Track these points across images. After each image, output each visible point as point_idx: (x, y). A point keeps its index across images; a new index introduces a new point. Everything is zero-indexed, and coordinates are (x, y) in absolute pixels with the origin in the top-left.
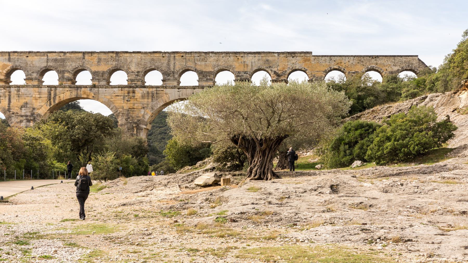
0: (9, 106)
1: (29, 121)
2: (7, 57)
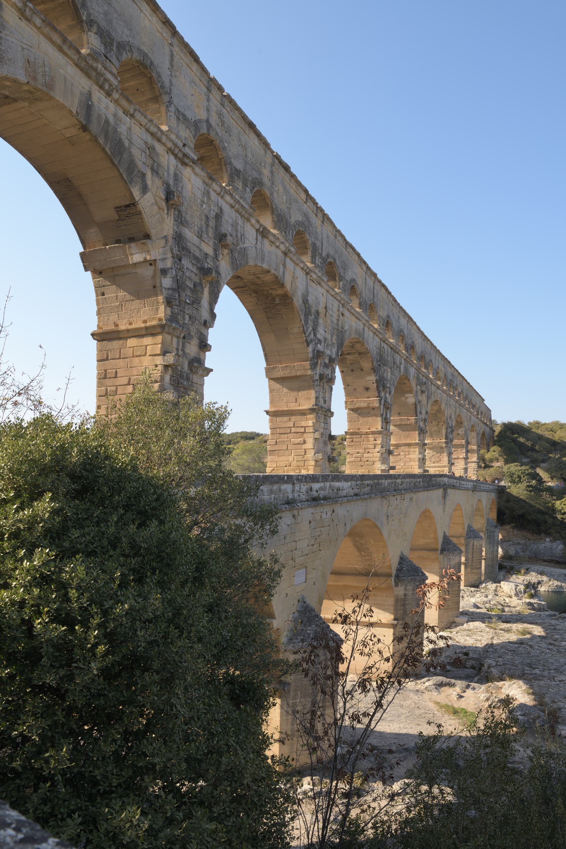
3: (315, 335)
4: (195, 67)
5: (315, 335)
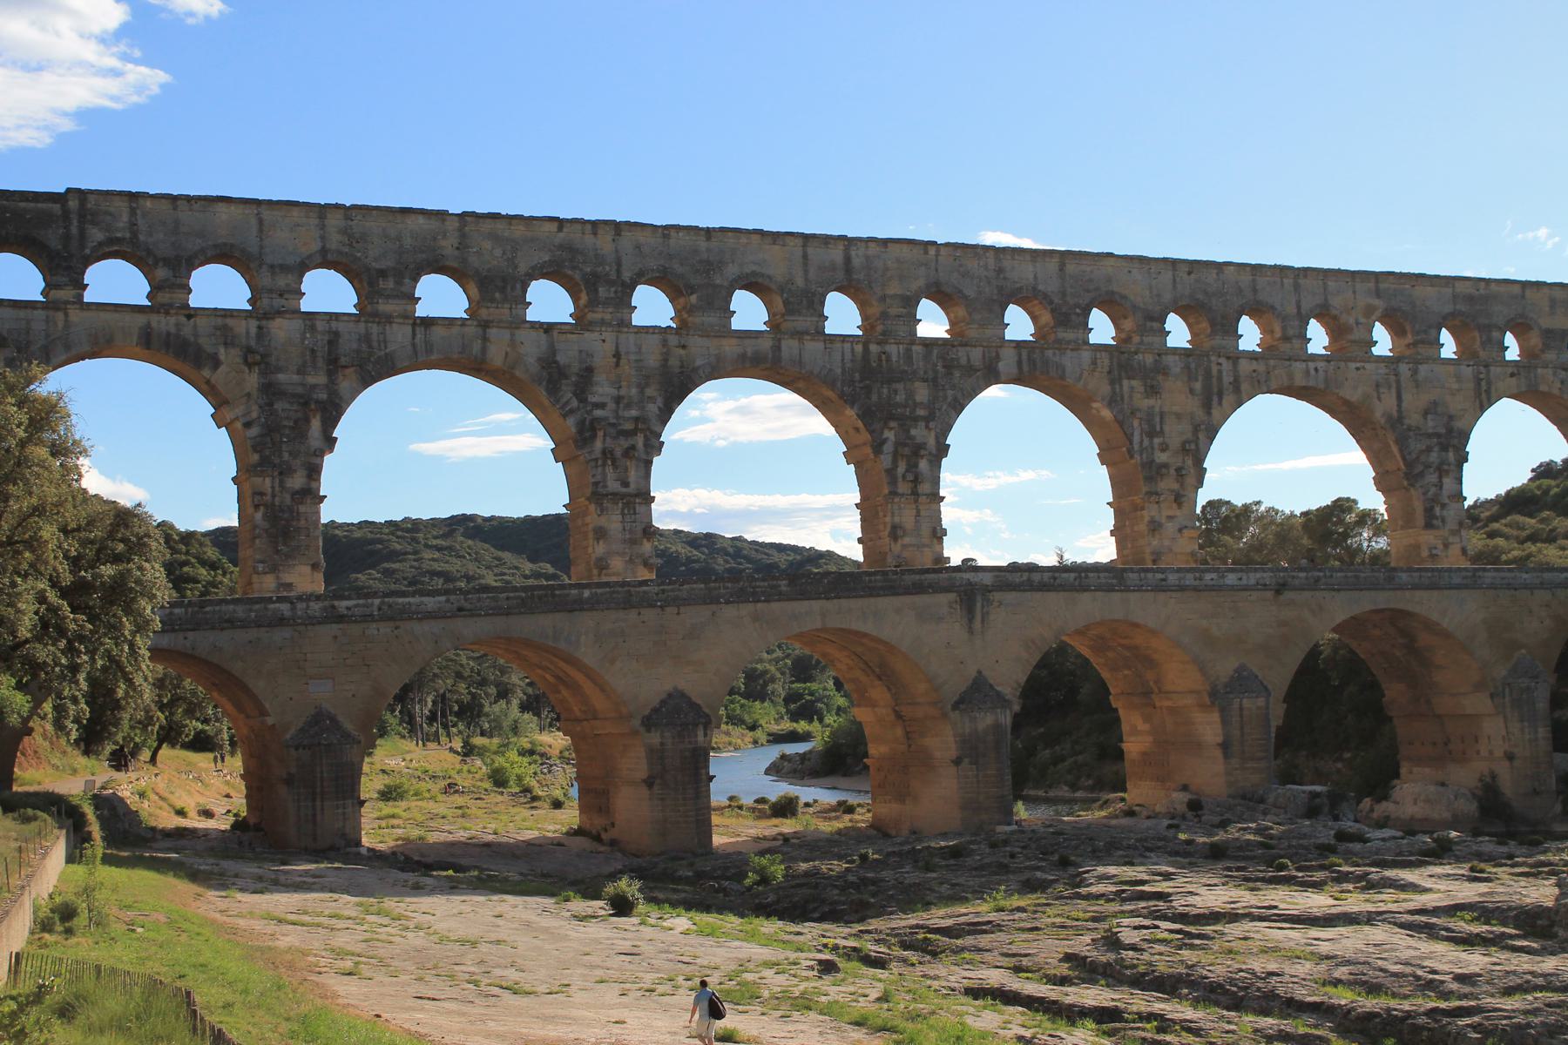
0: (1400, 411)
1: (1444, 448)
2: (1371, 285)
3: (583, 400)
4: (295, 212)
5: (583, 400)
